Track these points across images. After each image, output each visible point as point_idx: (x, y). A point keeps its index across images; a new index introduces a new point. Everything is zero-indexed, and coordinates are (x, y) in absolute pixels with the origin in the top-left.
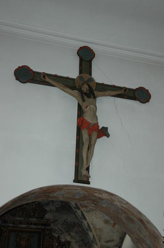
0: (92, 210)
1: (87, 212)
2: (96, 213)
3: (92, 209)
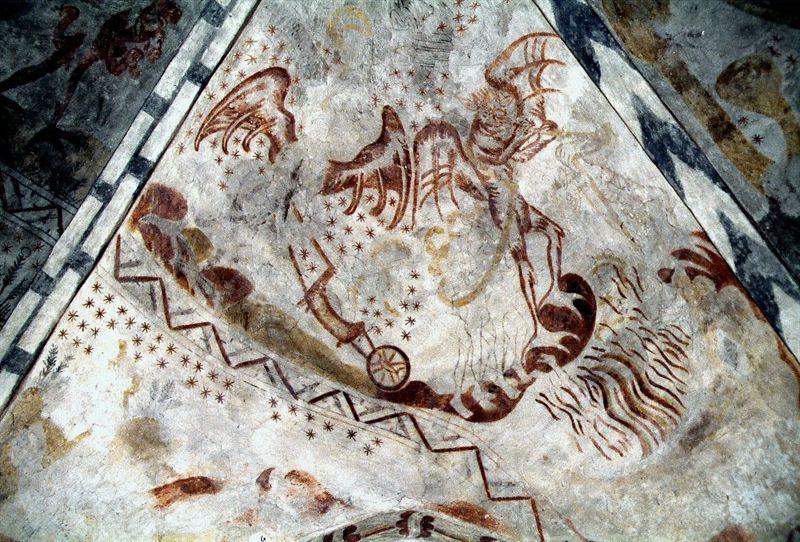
0: (152, 294)
1: (116, 277)
2: (149, 337)
3: (158, 290)
